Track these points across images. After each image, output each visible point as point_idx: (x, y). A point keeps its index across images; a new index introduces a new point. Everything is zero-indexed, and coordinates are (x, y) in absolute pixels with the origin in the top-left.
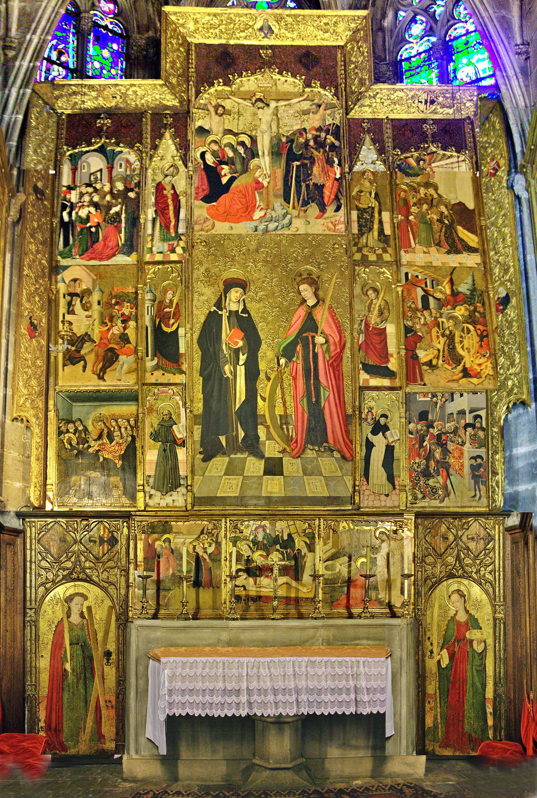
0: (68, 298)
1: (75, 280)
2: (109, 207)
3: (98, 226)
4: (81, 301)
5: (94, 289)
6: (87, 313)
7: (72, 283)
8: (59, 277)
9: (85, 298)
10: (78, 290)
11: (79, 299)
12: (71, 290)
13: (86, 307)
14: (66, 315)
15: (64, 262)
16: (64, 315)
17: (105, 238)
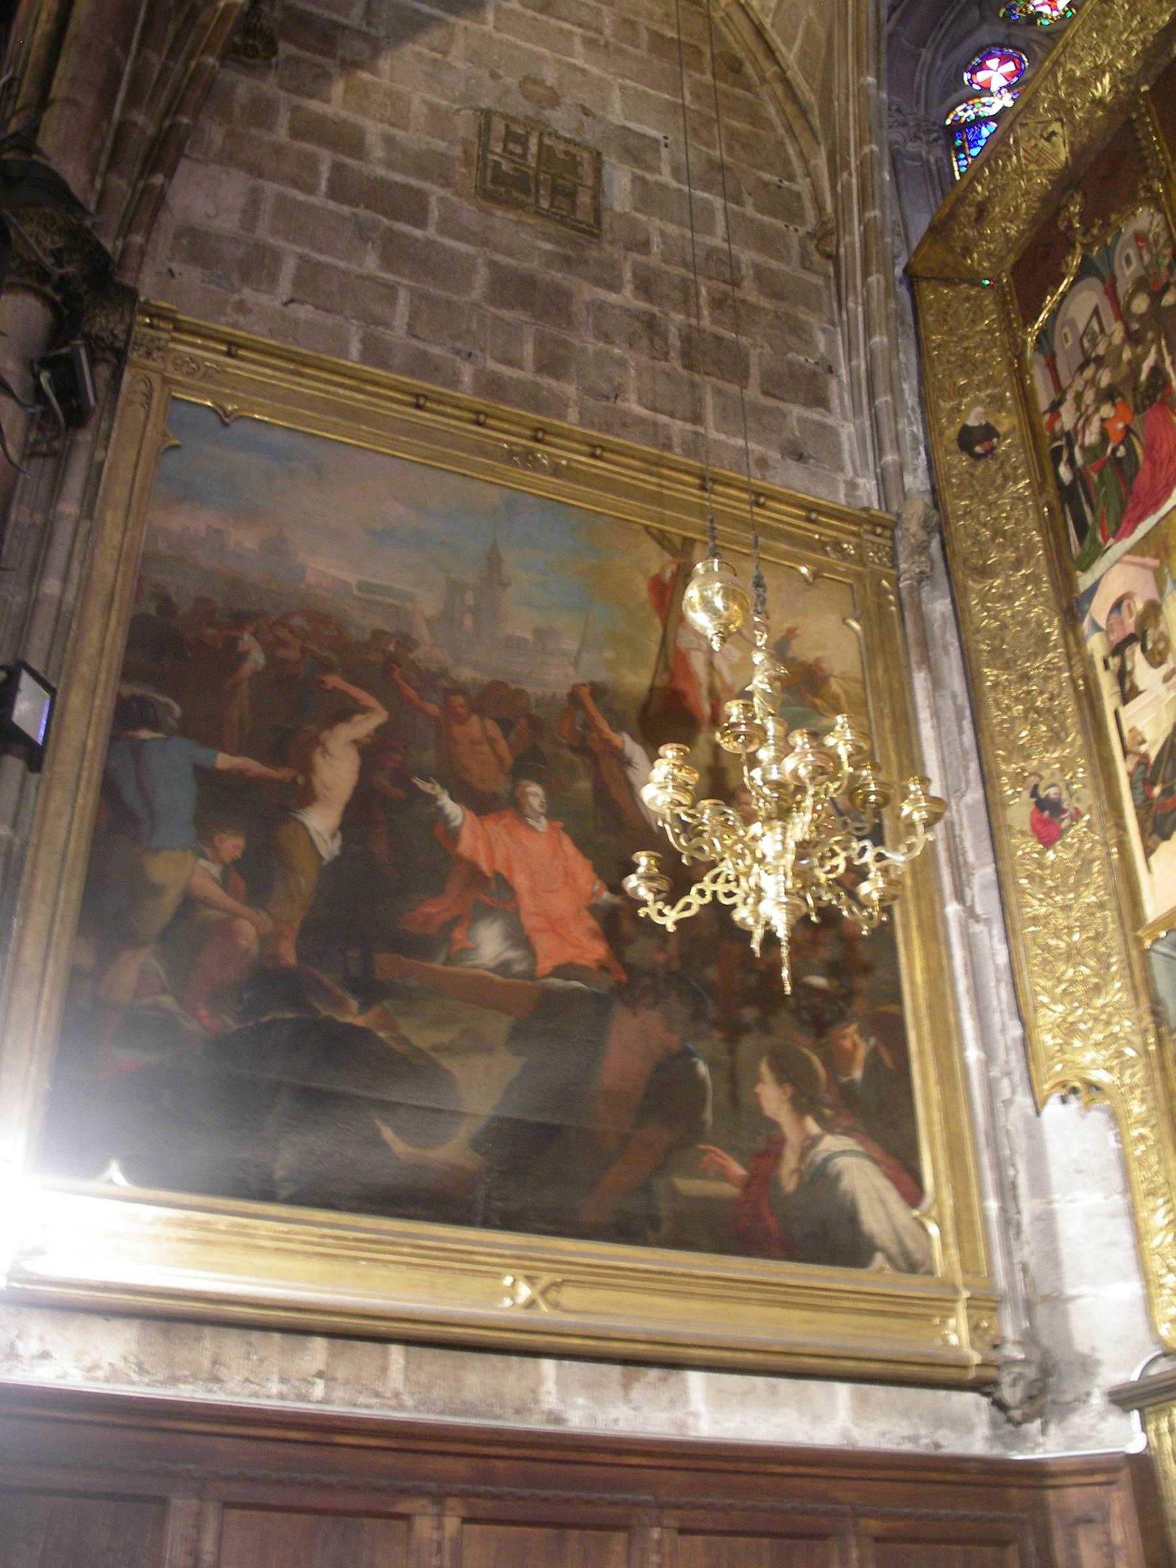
0: (1114, 662)
1: (1117, 606)
2: (1135, 365)
3: (1128, 430)
4: (1144, 649)
5: (1161, 592)
6: (1164, 669)
7: (1114, 615)
8: (1086, 625)
9: (1150, 632)
10: (1130, 625)
11: (1137, 648)
12: (1116, 637)
13: (1156, 659)
14: (1122, 710)
15: (1084, 581)
16: (1116, 714)
17: (1149, 449)
